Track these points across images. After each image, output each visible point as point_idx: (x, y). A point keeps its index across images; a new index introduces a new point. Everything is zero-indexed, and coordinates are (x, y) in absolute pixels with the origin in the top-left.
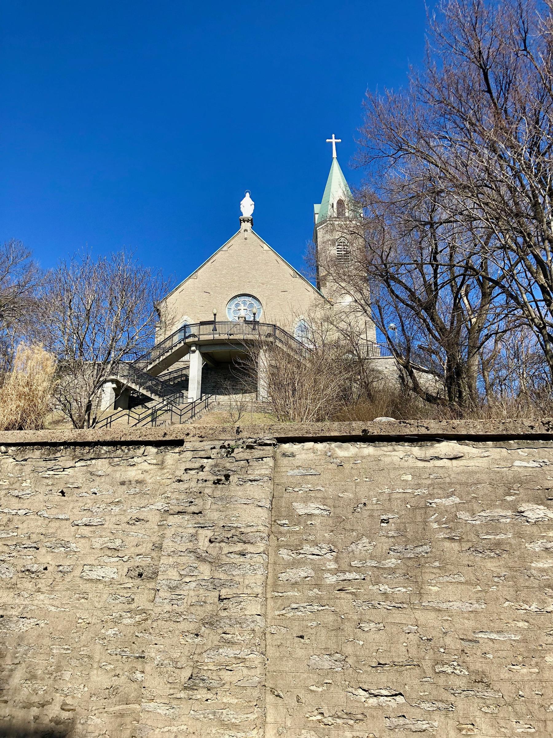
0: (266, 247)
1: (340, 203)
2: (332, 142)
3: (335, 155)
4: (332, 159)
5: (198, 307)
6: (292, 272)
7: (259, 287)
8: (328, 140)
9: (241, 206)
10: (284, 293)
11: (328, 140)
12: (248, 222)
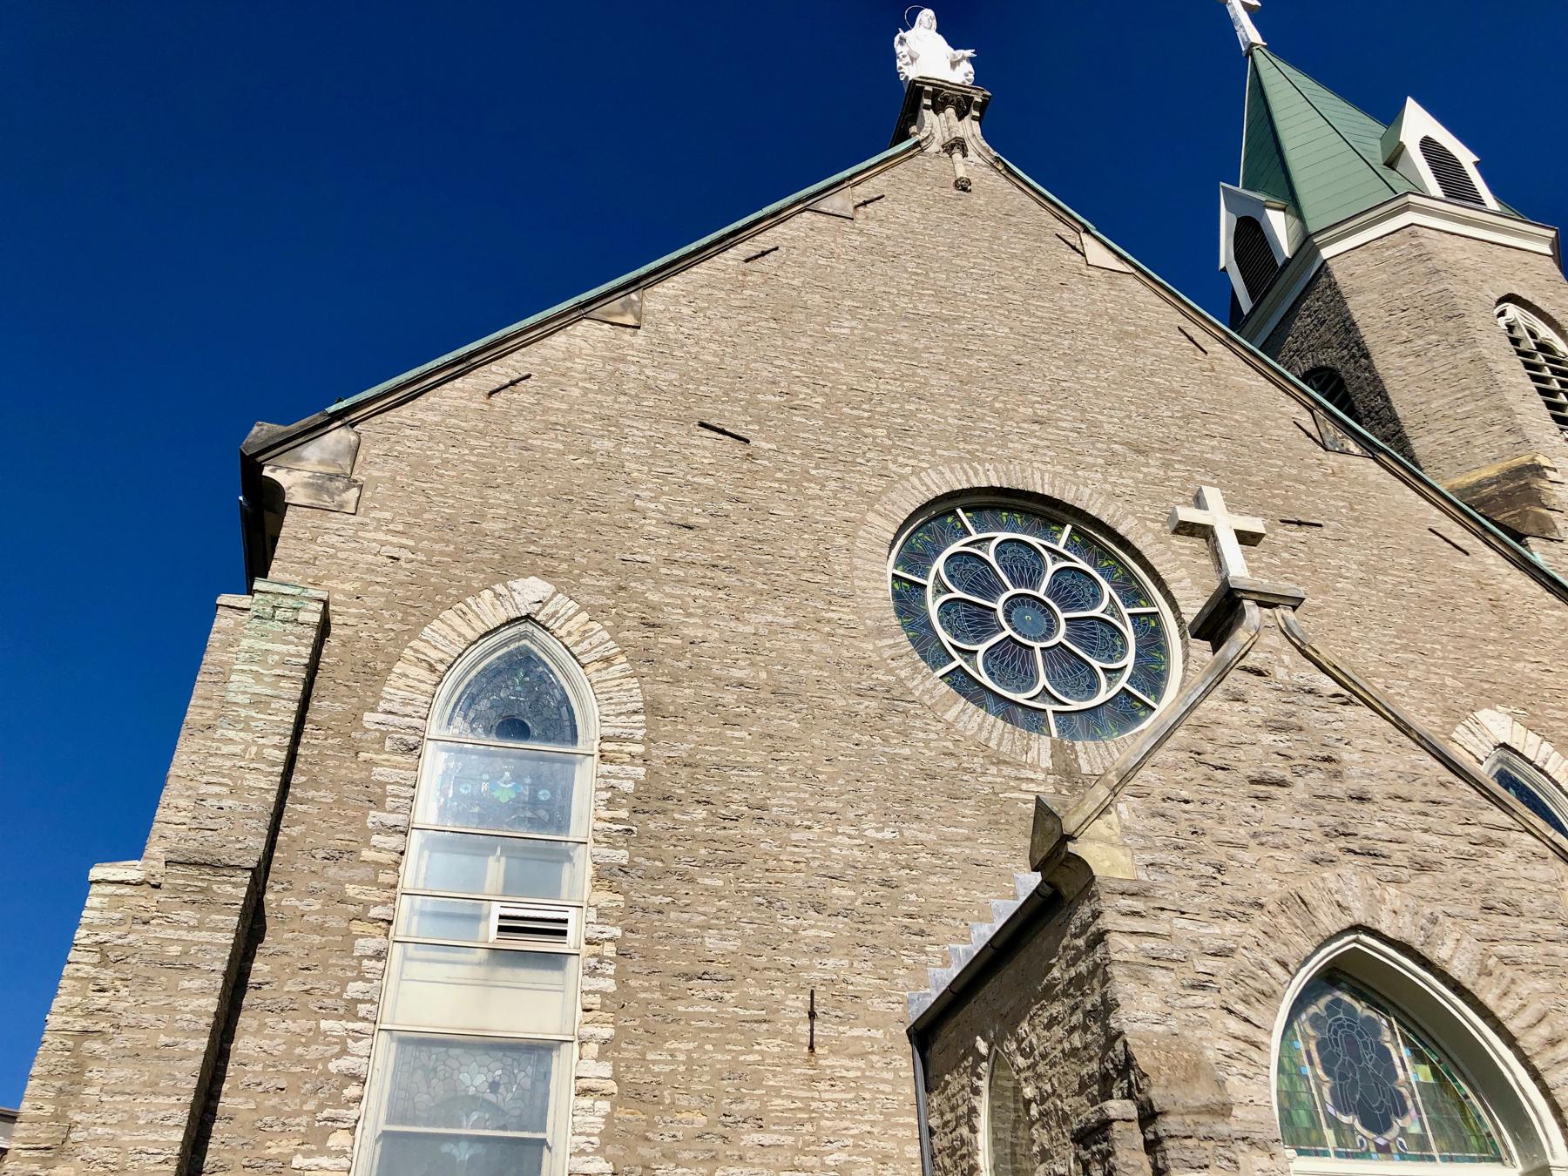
0: (1096, 252)
4: (1240, 58)
5: (650, 526)
6: (1306, 419)
10: (1300, 534)
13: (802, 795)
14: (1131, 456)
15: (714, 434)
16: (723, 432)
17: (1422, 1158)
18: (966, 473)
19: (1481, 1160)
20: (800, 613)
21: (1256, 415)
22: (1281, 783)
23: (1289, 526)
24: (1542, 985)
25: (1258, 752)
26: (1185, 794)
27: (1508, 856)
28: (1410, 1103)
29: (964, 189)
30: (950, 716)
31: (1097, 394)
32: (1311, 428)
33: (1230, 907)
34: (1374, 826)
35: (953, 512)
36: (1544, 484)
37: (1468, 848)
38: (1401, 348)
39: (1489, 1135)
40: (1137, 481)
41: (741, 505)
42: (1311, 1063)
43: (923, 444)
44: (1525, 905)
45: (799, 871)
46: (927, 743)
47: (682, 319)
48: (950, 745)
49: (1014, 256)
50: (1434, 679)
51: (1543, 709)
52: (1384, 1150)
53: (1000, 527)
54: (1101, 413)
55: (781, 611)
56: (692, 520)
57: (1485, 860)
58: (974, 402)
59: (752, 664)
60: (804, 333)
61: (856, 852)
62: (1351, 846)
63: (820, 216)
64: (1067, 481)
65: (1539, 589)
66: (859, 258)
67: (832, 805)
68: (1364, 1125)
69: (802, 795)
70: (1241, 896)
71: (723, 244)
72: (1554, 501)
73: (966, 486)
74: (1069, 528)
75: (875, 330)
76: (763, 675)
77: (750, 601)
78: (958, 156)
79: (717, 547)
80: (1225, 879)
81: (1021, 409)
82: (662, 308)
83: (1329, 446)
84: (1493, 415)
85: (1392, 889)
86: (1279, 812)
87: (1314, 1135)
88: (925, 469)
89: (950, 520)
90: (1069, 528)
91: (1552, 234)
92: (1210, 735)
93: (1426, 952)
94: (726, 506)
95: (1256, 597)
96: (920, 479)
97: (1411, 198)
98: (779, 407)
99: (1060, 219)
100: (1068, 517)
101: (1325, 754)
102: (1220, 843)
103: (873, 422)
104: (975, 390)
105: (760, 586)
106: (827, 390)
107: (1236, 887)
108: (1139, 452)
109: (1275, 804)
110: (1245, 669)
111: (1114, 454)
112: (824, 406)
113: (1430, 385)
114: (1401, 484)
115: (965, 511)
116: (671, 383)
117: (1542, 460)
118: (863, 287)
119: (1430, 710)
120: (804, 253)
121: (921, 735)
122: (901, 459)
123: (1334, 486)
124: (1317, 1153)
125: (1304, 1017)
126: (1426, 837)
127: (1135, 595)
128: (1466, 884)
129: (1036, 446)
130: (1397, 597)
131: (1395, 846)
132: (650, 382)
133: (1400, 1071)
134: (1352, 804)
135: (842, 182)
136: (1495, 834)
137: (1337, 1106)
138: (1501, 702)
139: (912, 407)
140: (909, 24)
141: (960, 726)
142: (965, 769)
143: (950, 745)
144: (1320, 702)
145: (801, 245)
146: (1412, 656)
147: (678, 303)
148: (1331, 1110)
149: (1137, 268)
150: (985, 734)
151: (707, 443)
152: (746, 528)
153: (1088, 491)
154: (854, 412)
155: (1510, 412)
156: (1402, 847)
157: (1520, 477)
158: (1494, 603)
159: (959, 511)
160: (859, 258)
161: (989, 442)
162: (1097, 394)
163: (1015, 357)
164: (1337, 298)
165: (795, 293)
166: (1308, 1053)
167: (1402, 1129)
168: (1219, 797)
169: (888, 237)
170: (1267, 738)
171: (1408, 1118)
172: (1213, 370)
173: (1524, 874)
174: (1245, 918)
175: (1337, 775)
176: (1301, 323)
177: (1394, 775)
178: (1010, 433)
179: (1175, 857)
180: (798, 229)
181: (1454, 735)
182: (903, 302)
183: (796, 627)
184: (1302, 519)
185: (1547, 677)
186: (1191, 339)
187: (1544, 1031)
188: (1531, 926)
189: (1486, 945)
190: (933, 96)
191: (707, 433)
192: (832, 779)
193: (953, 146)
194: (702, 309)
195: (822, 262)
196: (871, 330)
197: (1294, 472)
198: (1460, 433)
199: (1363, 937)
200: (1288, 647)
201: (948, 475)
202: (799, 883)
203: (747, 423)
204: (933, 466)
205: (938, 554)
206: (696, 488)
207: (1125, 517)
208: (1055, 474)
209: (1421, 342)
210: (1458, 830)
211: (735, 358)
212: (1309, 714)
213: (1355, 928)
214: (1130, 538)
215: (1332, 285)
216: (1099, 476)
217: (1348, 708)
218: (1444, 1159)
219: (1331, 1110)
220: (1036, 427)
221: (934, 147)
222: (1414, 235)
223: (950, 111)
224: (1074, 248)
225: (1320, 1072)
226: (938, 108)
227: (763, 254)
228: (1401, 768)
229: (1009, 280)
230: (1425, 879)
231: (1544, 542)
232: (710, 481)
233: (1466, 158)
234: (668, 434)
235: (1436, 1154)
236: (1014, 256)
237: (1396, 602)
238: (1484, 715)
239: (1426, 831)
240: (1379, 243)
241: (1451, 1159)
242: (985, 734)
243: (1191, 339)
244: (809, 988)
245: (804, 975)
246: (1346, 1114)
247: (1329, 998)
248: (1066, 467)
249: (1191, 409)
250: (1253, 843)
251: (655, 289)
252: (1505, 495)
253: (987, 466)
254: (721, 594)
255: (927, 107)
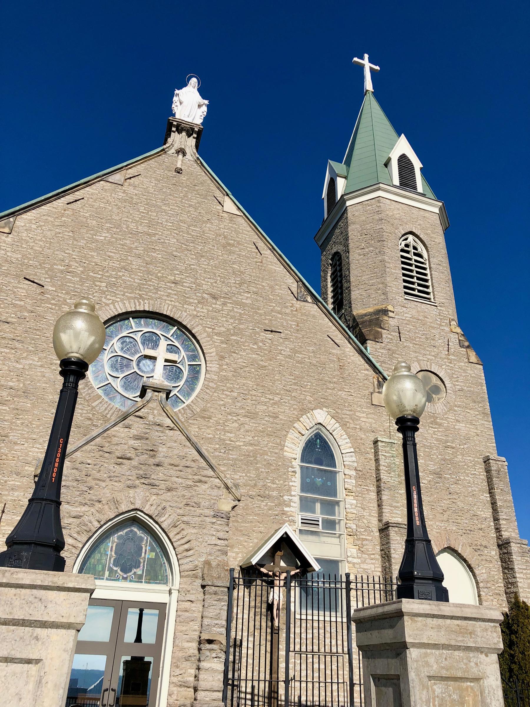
0: (230, 205)
1: (403, 160)
2: (362, 67)
3: (369, 85)
6: (294, 286)
7: (202, 302)
8: (356, 59)
9: (175, 99)
10: (270, 335)
11: (356, 59)
12: (189, 135)
13: (24, 432)
14: (210, 300)
15: (30, 283)
16: (33, 282)
17: (138, 582)
18: (135, 304)
19: (159, 583)
20: (45, 360)
21: (273, 283)
22: (129, 459)
23: (267, 332)
24: (194, 531)
25: (126, 447)
26: (89, 461)
27: (204, 487)
28: (142, 565)
29: (179, 173)
30: (94, 404)
31: (205, 271)
32: (294, 290)
33: (88, 501)
34: (158, 475)
35: (129, 319)
36: (386, 318)
37: (192, 484)
38: (360, 251)
39: (167, 576)
40: (208, 311)
41: (33, 314)
42: (111, 550)
43: (121, 291)
44: (203, 504)
45: (14, 460)
46: (81, 414)
47: (31, 230)
48: (91, 415)
49: (190, 206)
50: (302, 397)
51: (342, 410)
52: (125, 579)
53: (147, 325)
54: (204, 280)
55: (36, 359)
56: (10, 320)
57: (195, 488)
58: (149, 273)
59: (18, 381)
60: (83, 238)
61: (39, 454)
62: (145, 482)
63: (108, 184)
64: (178, 309)
65: (363, 362)
66: (119, 204)
67: (35, 436)
68: (121, 570)
69: (24, 432)
70: (94, 498)
71: (58, 196)
72: (387, 325)
73: (133, 309)
74: (176, 327)
75: (116, 238)
76: (22, 385)
77: (25, 355)
78: (181, 156)
79: (16, 332)
80: (91, 492)
81: (169, 277)
82: (23, 225)
83: (299, 298)
84: (381, 286)
85: (154, 497)
86: (125, 468)
87: (101, 573)
88: (118, 302)
89: (126, 322)
90: (176, 327)
91: (441, 204)
92: (109, 440)
93: (156, 519)
94: (26, 314)
95: (153, 389)
96: (114, 306)
97: (381, 185)
98: (62, 272)
99: (218, 188)
100: (176, 324)
101: (151, 449)
102: (95, 479)
103: (101, 280)
104: (151, 267)
105: (31, 348)
106: (85, 265)
107: (93, 495)
108: (214, 298)
109: (123, 466)
110: (135, 416)
111: (203, 298)
112: (82, 272)
113: (365, 269)
114: (324, 316)
115: (133, 318)
116: (17, 259)
117: (390, 308)
118: (117, 218)
119: (294, 409)
120: (95, 201)
121: (80, 411)
122: (108, 297)
123: (294, 315)
124: (100, 579)
125: (116, 535)
126: (177, 479)
127: (194, 357)
128: (184, 496)
129: (170, 293)
130: (301, 363)
131: (163, 482)
132: (9, 258)
133: (143, 554)
134: (153, 467)
135: (122, 168)
136: (204, 479)
137: (114, 565)
138: (326, 407)
139: (121, 274)
140: (183, 84)
141: (97, 408)
142: (94, 425)
143: (91, 415)
144: (161, 429)
145: (95, 197)
146: (296, 387)
147: (31, 223)
148: (111, 565)
149: (244, 214)
150: (107, 411)
151: (25, 286)
152: (32, 324)
153: (186, 314)
154: (95, 275)
155: (386, 286)
156: (166, 483)
157: (378, 314)
158: (341, 367)
159: (131, 319)
160: (119, 204)
161: (150, 291)
162: (205, 271)
163: (175, 253)
164: (347, 225)
165: (85, 220)
166: (112, 547)
167: (135, 572)
168: (101, 463)
169: (136, 195)
170: (132, 442)
171: (139, 569)
172: (262, 262)
173: (209, 493)
174: (93, 505)
175: (153, 456)
176: (337, 231)
177: (176, 457)
178: (161, 287)
179: (75, 484)
180: (96, 190)
181: (301, 419)
182: (132, 226)
183: (41, 366)
184: (274, 329)
185: (350, 398)
186: (257, 248)
187: (186, 546)
188: (201, 511)
189: (179, 517)
190: (177, 127)
191: (27, 282)
192: (38, 427)
193: (179, 152)
194: (41, 226)
195: (102, 205)
196: (114, 238)
197: (279, 309)
198: (368, 291)
199: (139, 512)
200: (159, 408)
201: (127, 304)
202: (13, 465)
203: (45, 278)
204: (122, 300)
205: (117, 336)
206: (15, 306)
207: (197, 326)
208: (174, 306)
209: (367, 250)
210: (190, 477)
211: (49, 249)
212: (155, 434)
213: (136, 509)
214: (196, 335)
215: (347, 218)
216: (193, 308)
217: (171, 431)
218: (146, 582)
219: (111, 565)
220: (173, 285)
221: (173, 151)
222: (379, 202)
223: (184, 134)
224: (220, 203)
225: (113, 553)
226: (179, 131)
227: (76, 201)
228: (180, 454)
229: (185, 217)
230: (169, 494)
231: (374, 343)
232: (22, 303)
233: (417, 165)
234: (10, 282)
235: (143, 581)
236: (190, 206)
237: (300, 365)
238: (317, 412)
239: (178, 477)
240: (367, 202)
241: (149, 583)
242: (107, 411)
243: (257, 248)
244: (5, 502)
245: (5, 497)
246: (116, 567)
247: (129, 529)
248: (180, 303)
249: (244, 280)
250: (108, 479)
251: (22, 216)
252: (370, 321)
253: (146, 301)
254: (13, 351)
255: (174, 132)
